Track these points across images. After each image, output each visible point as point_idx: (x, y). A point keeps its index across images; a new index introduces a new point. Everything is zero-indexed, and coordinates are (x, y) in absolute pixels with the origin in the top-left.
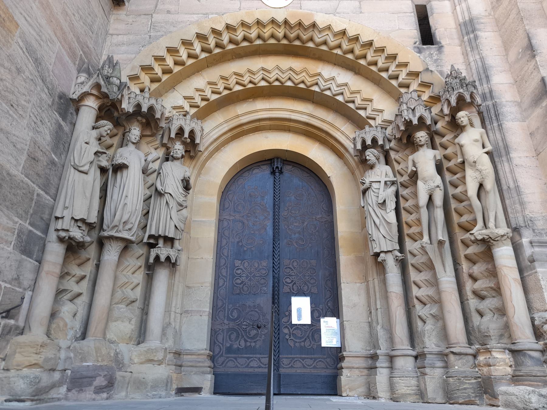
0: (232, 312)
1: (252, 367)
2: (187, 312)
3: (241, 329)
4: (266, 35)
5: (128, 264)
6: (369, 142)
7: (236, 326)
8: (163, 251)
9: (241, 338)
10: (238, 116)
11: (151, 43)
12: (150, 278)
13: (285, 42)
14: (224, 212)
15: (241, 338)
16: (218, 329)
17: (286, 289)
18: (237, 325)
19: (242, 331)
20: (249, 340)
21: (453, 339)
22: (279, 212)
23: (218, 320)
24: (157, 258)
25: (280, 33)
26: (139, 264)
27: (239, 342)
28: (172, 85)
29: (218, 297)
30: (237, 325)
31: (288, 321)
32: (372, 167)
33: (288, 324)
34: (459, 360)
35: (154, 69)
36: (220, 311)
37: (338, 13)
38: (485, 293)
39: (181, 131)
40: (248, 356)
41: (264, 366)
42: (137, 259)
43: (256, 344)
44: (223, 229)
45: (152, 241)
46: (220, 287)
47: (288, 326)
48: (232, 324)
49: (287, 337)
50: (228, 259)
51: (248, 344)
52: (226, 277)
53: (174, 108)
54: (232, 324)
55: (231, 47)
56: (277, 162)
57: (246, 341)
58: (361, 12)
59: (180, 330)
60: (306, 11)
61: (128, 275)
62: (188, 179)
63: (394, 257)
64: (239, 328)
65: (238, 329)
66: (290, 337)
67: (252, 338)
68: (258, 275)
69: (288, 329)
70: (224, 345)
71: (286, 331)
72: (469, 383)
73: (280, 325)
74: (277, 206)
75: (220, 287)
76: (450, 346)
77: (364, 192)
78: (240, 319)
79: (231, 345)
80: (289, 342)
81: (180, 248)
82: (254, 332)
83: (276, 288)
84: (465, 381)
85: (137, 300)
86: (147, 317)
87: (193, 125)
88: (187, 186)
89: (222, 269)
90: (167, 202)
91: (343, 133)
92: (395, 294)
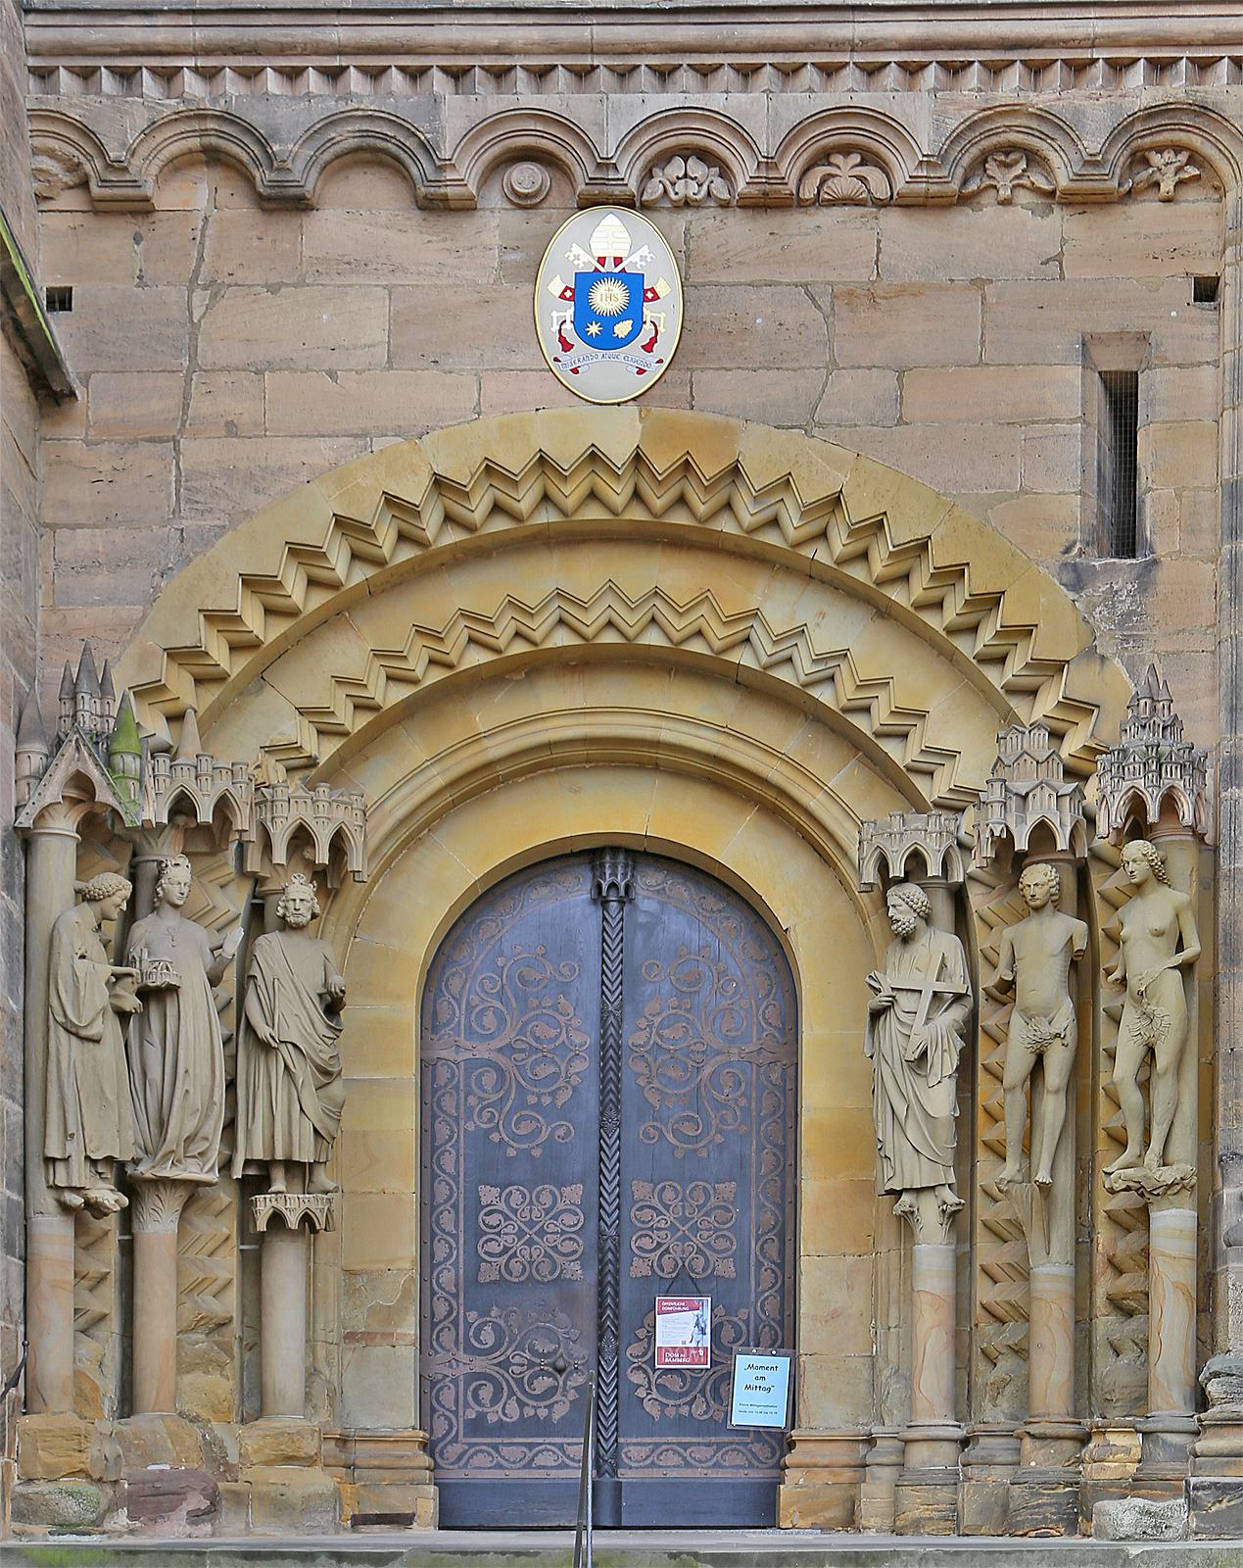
0: (479, 1329)
1: (539, 1467)
2: (350, 1337)
3: (506, 1375)
4: (570, 503)
5: (199, 1234)
6: (897, 870)
7: (497, 1368)
8: (285, 1199)
9: (509, 1398)
10: (477, 739)
11: (188, 560)
12: (253, 1266)
13: (637, 514)
14: (436, 1038)
15: (509, 1398)
16: (441, 1377)
17: (638, 1268)
18: (494, 1365)
19: (510, 1380)
20: (531, 1403)
21: (1038, 1405)
22: (619, 1058)
23: (437, 1352)
24: (277, 1219)
25: (618, 493)
26: (225, 1231)
27: (504, 1408)
28: (259, 678)
29: (433, 1293)
30: (494, 1365)
31: (644, 1354)
32: (906, 939)
33: (644, 1359)
34: (1041, 1448)
35: (207, 653)
36: (442, 1330)
37: (820, 425)
38: (1132, 1303)
39: (302, 838)
40: (530, 1440)
41: (576, 1465)
42: (216, 1216)
43: (550, 1413)
44: (437, 1090)
45: (251, 1172)
46: (440, 1264)
47: (644, 1366)
48: (480, 1364)
49: (641, 1393)
50: (457, 1184)
51: (529, 1412)
52: (456, 1237)
53: (270, 750)
54: (480, 1364)
55: (453, 536)
56: (614, 867)
57: (521, 1405)
58: (900, 421)
59: (340, 1383)
60: (712, 417)
61: (202, 1261)
62: (341, 994)
63: (940, 1203)
64: (502, 1371)
65: (498, 1376)
66: (648, 1394)
67: (536, 1398)
68: (552, 1228)
69: (645, 1372)
70: (461, 1413)
71: (637, 1378)
72: (1049, 1495)
73: (621, 1363)
74: (611, 1018)
75: (440, 1264)
76: (1032, 1420)
77: (876, 1015)
78: (502, 1350)
79: (481, 1416)
80: (648, 1406)
81: (331, 1185)
82: (543, 1384)
83: (609, 1278)
84: (1041, 1491)
85: (231, 1320)
86: (260, 1355)
87: (340, 815)
88: (333, 1006)
89: (441, 1213)
90: (286, 1067)
91: (832, 796)
92: (929, 1296)
